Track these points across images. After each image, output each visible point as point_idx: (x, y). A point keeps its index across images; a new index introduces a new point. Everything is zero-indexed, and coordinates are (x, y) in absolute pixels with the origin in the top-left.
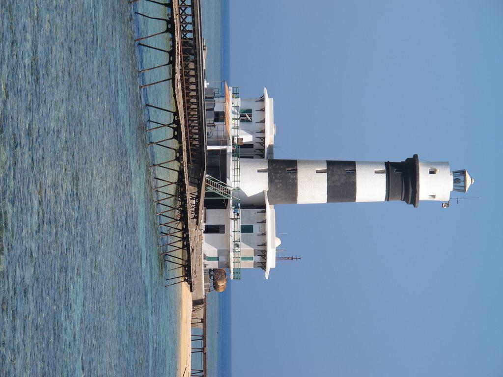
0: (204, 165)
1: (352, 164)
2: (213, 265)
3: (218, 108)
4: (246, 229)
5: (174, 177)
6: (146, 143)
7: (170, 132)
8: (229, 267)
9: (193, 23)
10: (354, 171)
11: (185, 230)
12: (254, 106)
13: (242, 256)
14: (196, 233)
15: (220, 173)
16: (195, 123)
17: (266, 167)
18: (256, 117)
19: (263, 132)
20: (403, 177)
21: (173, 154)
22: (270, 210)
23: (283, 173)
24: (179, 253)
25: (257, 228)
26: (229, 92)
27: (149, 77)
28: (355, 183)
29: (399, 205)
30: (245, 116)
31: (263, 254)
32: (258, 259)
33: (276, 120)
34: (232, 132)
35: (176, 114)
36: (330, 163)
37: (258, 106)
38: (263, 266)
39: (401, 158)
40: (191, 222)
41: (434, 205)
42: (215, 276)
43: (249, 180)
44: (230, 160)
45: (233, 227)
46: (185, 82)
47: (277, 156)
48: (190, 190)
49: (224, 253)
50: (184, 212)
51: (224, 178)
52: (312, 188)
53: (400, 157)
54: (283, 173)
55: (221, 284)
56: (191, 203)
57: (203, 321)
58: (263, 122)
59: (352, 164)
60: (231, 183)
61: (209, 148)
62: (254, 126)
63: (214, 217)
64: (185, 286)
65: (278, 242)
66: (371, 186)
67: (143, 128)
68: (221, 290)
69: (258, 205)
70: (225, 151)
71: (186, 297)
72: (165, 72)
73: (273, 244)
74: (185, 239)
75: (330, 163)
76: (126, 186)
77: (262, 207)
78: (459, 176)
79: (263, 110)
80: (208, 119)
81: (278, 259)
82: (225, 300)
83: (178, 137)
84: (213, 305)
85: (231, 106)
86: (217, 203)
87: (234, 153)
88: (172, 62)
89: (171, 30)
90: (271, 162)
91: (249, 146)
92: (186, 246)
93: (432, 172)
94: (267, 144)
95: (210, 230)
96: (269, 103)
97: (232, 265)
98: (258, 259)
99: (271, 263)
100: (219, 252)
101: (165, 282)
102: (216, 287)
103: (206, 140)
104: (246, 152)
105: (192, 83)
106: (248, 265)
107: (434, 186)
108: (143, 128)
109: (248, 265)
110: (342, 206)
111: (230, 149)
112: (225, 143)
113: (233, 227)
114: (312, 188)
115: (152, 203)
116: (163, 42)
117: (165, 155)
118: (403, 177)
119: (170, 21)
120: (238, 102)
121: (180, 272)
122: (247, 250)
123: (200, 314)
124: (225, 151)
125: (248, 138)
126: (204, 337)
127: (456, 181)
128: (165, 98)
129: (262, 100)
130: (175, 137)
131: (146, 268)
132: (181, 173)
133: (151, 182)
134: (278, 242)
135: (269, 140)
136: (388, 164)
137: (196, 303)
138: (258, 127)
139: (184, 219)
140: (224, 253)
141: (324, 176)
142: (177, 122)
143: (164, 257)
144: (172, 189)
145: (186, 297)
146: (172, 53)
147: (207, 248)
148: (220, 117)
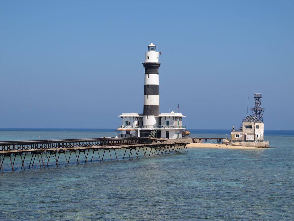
0: (145, 138)
1: (145, 86)
2: (180, 135)
3: (125, 133)
4: (168, 123)
5: (149, 149)
6: (138, 159)
7: (133, 150)
8: (181, 130)
9: (95, 141)
11: (168, 145)
12: (125, 120)
13: (177, 125)
14: (169, 141)
15: (148, 132)
17: (146, 116)
18: (128, 120)
19: (134, 117)
20: (150, 68)
21: (141, 149)
24: (176, 147)
25: (168, 120)
26: (120, 129)
27: (114, 157)
28: (152, 85)
29: (160, 69)
30: (128, 124)
31: (177, 118)
32: (178, 120)
34: (134, 128)
35: (127, 148)
36: (145, 94)
38: (181, 118)
40: (165, 143)
41: (160, 58)
42: (184, 135)
43: (151, 123)
45: (167, 128)
48: (154, 143)
49: (176, 131)
50: (161, 145)
51: (150, 131)
52: (154, 100)
54: (148, 110)
55: (187, 133)
56: (158, 143)
57: (200, 139)
58: (130, 117)
59: (145, 86)
60: (151, 129)
61: (139, 136)
62: (132, 120)
63: (163, 135)
64: (188, 145)
65: (173, 112)
66: (153, 79)
67: (131, 159)
69: (159, 119)
70: (140, 131)
71: (191, 145)
72: (112, 152)
73: (173, 114)
74: (171, 145)
75: (145, 94)
77: (160, 118)
78: (150, 48)
79: (126, 117)
80: (129, 136)
81: (178, 112)
82: (192, 131)
83: (135, 147)
84: (195, 136)
85: (124, 128)
86: (158, 134)
87: (141, 127)
88: (109, 149)
89: (97, 149)
90: (144, 114)
92: (174, 145)
93: (149, 58)
94: (138, 116)
95: (168, 136)
96: (124, 115)
97: (180, 129)
98: (178, 120)
99: (180, 115)
100: (176, 133)
101: (186, 153)
102: (188, 135)
104: (141, 123)
105: (116, 142)
106: (180, 123)
107: (153, 57)
108: (131, 159)
109: (180, 123)
111: (140, 129)
112: (138, 131)
113: (167, 128)
114: (154, 100)
115: (158, 157)
116: (101, 152)
117: (141, 152)
118: (150, 68)
119: (94, 149)
120: (123, 126)
121: (183, 147)
122: (175, 123)
123: (198, 140)
124: (140, 131)
125: (136, 123)
126: (206, 139)
127: (152, 50)
128: (121, 152)
129: (122, 117)
130: (135, 148)
132: (148, 146)
133: (150, 157)
134: (173, 112)
135: (137, 115)
136: (146, 73)
137: (194, 142)
138: (132, 119)
139: (164, 146)
140: (176, 131)
141: (149, 96)
142: (130, 147)
143: (178, 153)
144: (153, 150)
145: (191, 145)
146: (105, 149)
147: (174, 138)
148: (128, 132)
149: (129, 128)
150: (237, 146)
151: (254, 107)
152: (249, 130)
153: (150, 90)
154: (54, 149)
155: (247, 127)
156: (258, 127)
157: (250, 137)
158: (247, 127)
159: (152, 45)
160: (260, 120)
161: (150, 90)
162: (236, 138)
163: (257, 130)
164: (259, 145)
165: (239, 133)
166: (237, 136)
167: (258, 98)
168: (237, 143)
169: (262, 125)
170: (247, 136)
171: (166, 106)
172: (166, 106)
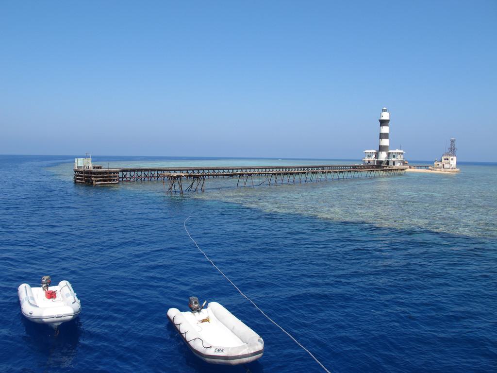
0: (379, 165)
2: (402, 164)
3: (367, 162)
4: (394, 157)
5: (382, 172)
6: (375, 177)
7: (372, 172)
10: (382, 133)
11: (394, 170)
12: (367, 154)
13: (400, 158)
14: (394, 167)
15: (381, 162)
16: (370, 167)
20: (383, 123)
21: (377, 172)
22: (390, 151)
23: (382, 148)
24: (399, 171)
26: (364, 159)
27: (360, 176)
30: (369, 156)
31: (400, 153)
34: (373, 159)
36: (380, 138)
38: (402, 153)
40: (392, 168)
41: (390, 116)
42: (404, 164)
43: (383, 156)
44: (378, 160)
45: (394, 159)
46: (361, 169)
47: (378, 150)
48: (385, 168)
50: (390, 170)
52: (385, 142)
54: (382, 148)
55: (406, 162)
56: (388, 168)
57: (414, 166)
59: (380, 134)
60: (384, 160)
62: (371, 154)
63: (391, 163)
64: (406, 170)
65: (397, 150)
66: (385, 130)
67: (371, 178)
69: (389, 154)
71: (409, 170)
72: (359, 173)
73: (397, 151)
74: (396, 170)
75: (380, 138)
76: (384, 182)
77: (389, 153)
78: (383, 111)
80: (370, 164)
82: (410, 162)
83: (373, 171)
84: (411, 164)
85: (367, 159)
86: (388, 163)
88: (357, 171)
89: (350, 171)
90: (379, 151)
92: (397, 170)
95: (394, 165)
99: (402, 151)
100: (399, 162)
101: (405, 175)
102: (407, 164)
104: (377, 156)
106: (402, 156)
107: (385, 116)
108: (371, 178)
109: (402, 156)
111: (376, 160)
113: (394, 159)
114: (385, 142)
115: (388, 177)
116: (353, 173)
117: (377, 174)
118: (383, 123)
119: (348, 171)
121: (403, 171)
125: (374, 156)
128: (365, 173)
131: (402, 178)
132: (381, 170)
133: (383, 177)
134: (397, 150)
135: (375, 151)
137: (410, 168)
139: (391, 170)
140: (399, 161)
141: (383, 140)
142: (370, 171)
143: (400, 175)
144: (384, 172)
145: (409, 170)
146: (355, 171)
147: (398, 165)
148: (369, 162)
149: (370, 159)
150: (438, 171)
151: (450, 146)
152: (446, 161)
153: (383, 136)
154: (325, 171)
155: (445, 159)
156: (452, 159)
157: (446, 166)
158: (445, 159)
159: (385, 109)
160: (454, 155)
161: (383, 136)
162: (438, 166)
163: (451, 161)
164: (452, 171)
165: (439, 163)
166: (438, 165)
167: (453, 141)
168: (439, 169)
169: (455, 158)
170: (445, 165)
171: (393, 145)
172: (393, 145)
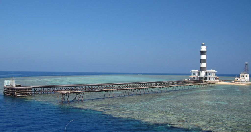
1: (201, 60)
2: (215, 79)
3: (193, 78)
4: (210, 74)
5: (203, 85)
8: (215, 77)
9: (181, 81)
10: (202, 59)
15: (201, 78)
17: (201, 71)
18: (194, 73)
19: (196, 72)
20: (202, 53)
22: (207, 71)
23: (202, 69)
25: (209, 73)
28: (203, 59)
29: (206, 53)
30: (194, 74)
31: (213, 72)
32: (214, 73)
33: (195, 70)
34: (196, 76)
35: (198, 85)
37: (193, 72)
38: (215, 72)
39: (200, 53)
43: (203, 74)
44: (200, 76)
45: (209, 76)
47: (199, 70)
49: (213, 77)
51: (202, 77)
53: (200, 53)
54: (202, 69)
57: (222, 81)
58: (195, 72)
60: (203, 76)
61: (198, 79)
62: (195, 73)
63: (208, 79)
65: (212, 70)
66: (204, 57)
68: (219, 78)
69: (206, 73)
70: (199, 77)
73: (212, 71)
77: (206, 72)
78: (203, 45)
79: (193, 72)
80: (194, 79)
81: (214, 70)
85: (192, 76)
87: (199, 76)
90: (200, 71)
91: (198, 74)
93: (202, 49)
94: (198, 71)
96: (192, 71)
97: (215, 76)
98: (214, 73)
99: (214, 71)
102: (218, 79)
103: (197, 80)
104: (199, 74)
105: (148, 84)
106: (215, 74)
107: (204, 48)
108: (191, 90)
110: (206, 61)
111: (198, 76)
112: (198, 77)
113: (209, 76)
114: (204, 65)
118: (202, 53)
120: (192, 75)
122: (212, 74)
123: (222, 81)
124: (199, 77)
125: (197, 74)
126: (225, 81)
127: (203, 45)
128: (187, 86)
129: (192, 72)
130: (128, 90)
134: (212, 70)
135: (197, 71)
136: (201, 55)
137: (220, 81)
138: (211, 72)
140: (213, 77)
148: (194, 78)
149: (194, 76)
150: (237, 84)
151: (245, 68)
152: (243, 77)
153: (203, 61)
154: (160, 86)
155: (242, 76)
156: (246, 76)
157: (243, 80)
158: (242, 76)
159: (203, 44)
160: (247, 73)
161: (203, 61)
162: (237, 80)
163: (246, 77)
164: (247, 83)
165: (238, 79)
166: (238, 80)
167: (246, 65)
168: (238, 83)
169: (248, 75)
171: (209, 67)
172: (209, 67)
